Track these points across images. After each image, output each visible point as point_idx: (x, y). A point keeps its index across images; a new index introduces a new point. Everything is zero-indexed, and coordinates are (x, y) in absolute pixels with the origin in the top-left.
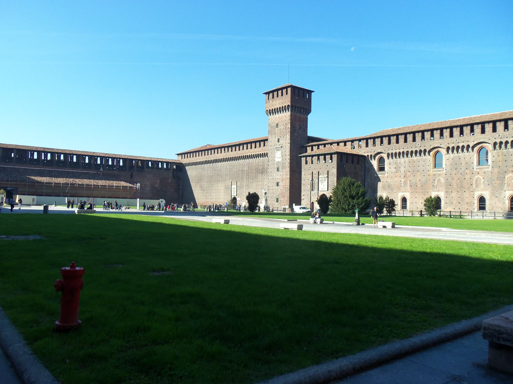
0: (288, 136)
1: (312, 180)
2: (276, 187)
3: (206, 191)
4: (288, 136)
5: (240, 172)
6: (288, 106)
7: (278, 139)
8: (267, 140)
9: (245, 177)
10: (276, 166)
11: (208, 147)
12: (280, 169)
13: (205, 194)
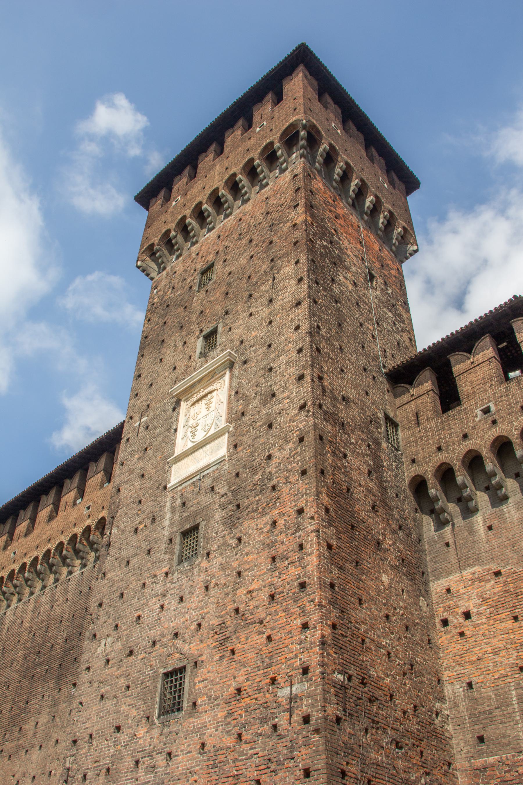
4: (288, 269)
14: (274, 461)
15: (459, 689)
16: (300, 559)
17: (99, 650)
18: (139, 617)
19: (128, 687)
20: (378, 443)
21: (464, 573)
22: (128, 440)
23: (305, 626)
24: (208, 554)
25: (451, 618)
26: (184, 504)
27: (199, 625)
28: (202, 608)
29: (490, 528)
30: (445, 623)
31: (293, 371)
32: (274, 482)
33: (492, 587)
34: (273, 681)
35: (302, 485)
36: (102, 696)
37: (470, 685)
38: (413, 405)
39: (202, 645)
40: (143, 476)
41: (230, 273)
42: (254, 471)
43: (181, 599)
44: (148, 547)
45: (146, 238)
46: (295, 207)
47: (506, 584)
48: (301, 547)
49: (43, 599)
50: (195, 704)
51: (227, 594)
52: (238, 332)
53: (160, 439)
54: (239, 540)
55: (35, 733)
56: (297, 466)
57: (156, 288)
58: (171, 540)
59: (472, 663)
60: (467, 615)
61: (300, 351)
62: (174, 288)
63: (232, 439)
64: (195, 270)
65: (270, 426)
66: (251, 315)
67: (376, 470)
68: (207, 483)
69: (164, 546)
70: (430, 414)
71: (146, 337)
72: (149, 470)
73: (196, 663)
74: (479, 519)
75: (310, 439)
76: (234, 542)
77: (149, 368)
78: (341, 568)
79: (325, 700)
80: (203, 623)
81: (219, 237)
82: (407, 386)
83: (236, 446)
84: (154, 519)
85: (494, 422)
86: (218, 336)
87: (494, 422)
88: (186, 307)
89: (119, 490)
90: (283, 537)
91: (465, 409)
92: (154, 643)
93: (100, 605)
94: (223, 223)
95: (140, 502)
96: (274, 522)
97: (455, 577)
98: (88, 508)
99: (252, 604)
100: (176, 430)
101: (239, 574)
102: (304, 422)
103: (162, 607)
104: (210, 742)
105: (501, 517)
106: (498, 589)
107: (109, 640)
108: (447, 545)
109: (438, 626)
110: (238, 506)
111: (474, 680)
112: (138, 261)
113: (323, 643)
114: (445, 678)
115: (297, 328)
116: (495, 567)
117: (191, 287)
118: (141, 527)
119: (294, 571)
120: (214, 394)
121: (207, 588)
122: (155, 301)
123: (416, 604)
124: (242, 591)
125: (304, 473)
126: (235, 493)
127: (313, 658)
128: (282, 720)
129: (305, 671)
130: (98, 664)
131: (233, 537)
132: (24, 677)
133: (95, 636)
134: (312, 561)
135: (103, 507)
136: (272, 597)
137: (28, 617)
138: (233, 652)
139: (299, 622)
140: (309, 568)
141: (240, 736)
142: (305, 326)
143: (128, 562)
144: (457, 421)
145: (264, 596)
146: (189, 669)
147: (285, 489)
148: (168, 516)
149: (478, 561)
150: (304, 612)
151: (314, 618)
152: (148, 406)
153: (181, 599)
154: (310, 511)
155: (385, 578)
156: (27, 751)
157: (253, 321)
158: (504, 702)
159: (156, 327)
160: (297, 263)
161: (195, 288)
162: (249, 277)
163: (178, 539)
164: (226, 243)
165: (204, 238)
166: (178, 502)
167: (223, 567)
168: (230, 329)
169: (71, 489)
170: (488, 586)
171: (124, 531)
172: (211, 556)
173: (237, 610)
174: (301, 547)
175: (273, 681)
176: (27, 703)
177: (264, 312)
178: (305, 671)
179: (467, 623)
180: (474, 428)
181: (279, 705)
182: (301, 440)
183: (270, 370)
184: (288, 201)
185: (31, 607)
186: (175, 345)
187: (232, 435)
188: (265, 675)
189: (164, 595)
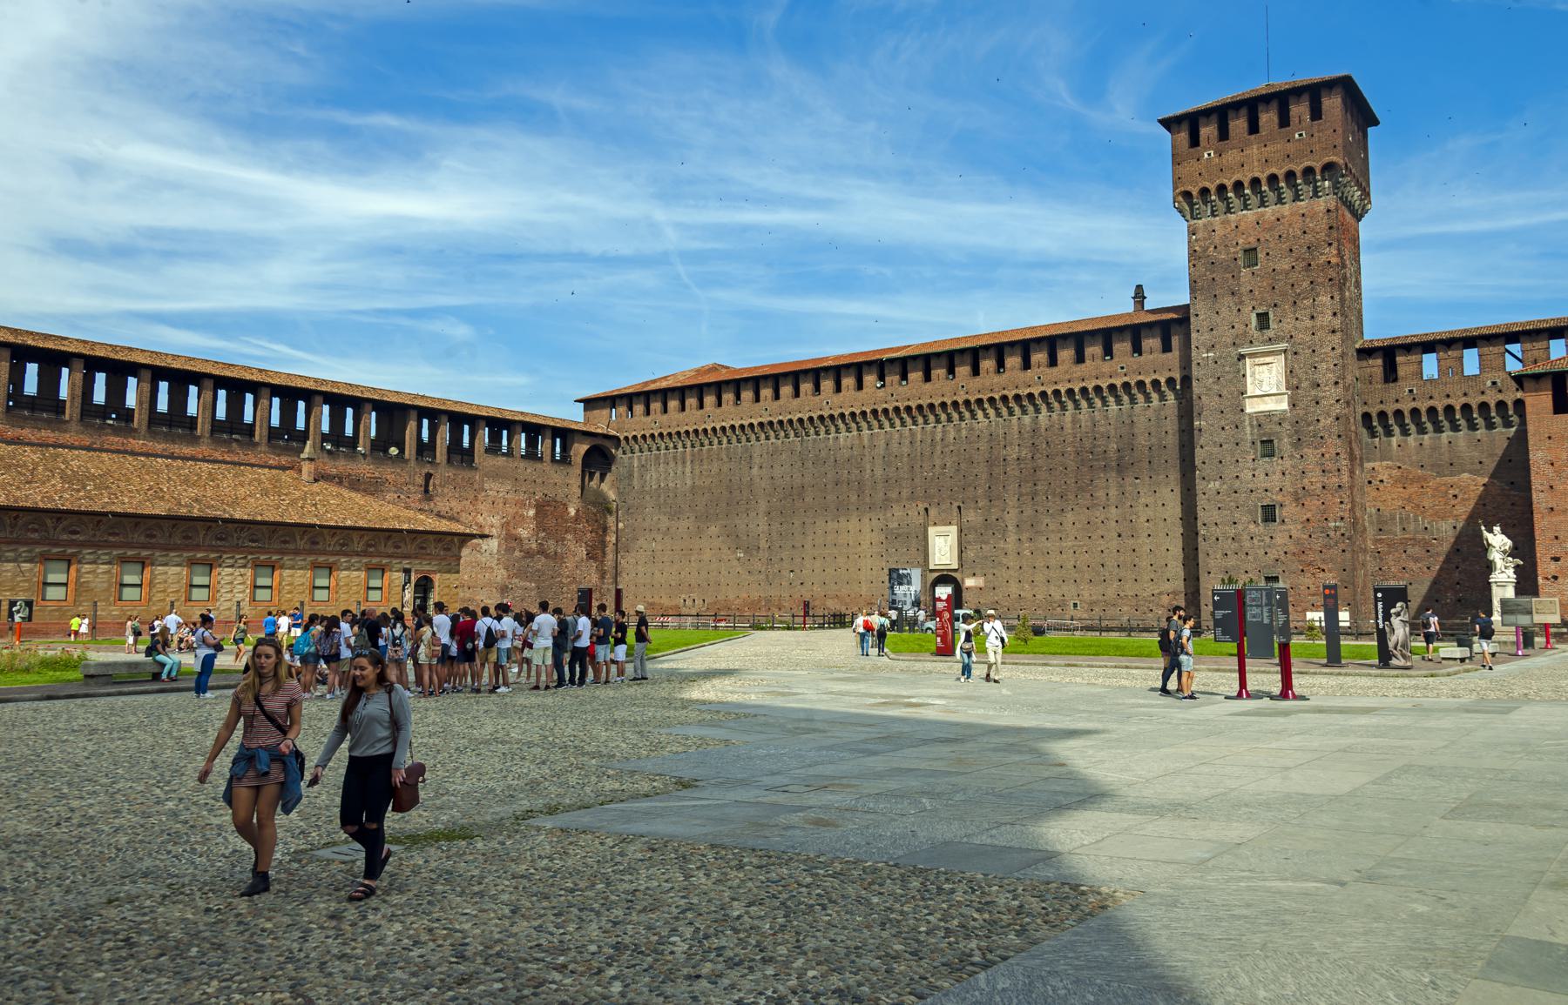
0: (1324, 299)
2: (1260, 529)
3: (764, 555)
4: (1324, 299)
5: (982, 470)
6: (1329, 167)
9: (1013, 487)
10: (1248, 433)
11: (724, 376)
12: (1284, 444)
13: (758, 566)
31: (1332, 377)
33: (1395, 472)
45: (1177, 180)
52: (1288, 325)
56: (1335, 430)
68: (1276, 419)
72: (1224, 393)
74: (1394, 440)
126: (1296, 432)
127: (1346, 515)
128: (1332, 534)
134: (1345, 478)
144: (1393, 390)
145: (1319, 485)
149: (1390, 459)
154: (1343, 456)
158: (1393, 518)
161: (1240, 262)
177: (1309, 323)
187: (1290, 398)
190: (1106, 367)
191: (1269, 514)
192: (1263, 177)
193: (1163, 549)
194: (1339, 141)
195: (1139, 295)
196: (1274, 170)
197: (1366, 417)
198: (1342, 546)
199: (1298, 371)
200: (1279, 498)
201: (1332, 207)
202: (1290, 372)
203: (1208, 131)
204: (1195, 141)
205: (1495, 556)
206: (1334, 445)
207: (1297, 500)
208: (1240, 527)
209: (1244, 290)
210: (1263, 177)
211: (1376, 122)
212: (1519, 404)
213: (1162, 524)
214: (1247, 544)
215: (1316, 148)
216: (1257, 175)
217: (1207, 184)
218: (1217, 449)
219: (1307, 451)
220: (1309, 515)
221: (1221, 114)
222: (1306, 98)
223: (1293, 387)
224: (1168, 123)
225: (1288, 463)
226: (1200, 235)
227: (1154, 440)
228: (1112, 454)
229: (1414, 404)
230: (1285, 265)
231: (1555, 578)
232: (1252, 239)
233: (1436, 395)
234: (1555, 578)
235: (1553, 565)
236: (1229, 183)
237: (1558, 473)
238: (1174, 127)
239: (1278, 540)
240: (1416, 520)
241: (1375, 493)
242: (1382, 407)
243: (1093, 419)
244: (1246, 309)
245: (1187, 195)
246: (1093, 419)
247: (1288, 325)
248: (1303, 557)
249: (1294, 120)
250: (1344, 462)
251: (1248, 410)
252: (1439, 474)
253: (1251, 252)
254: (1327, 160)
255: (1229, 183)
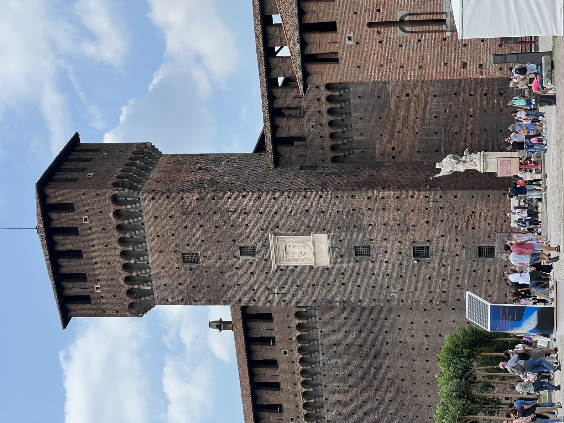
0: (230, 204)
1: (401, 23)
4: (230, 204)
6: (115, 199)
7: (244, 250)
8: (244, 308)
10: (348, 265)
12: (358, 238)
14: (341, 210)
15: (419, 155)
16: (388, 198)
17: (396, 296)
18: (387, 275)
19: (415, 275)
20: (320, 173)
21: (376, 147)
22: (284, 301)
23: (412, 197)
24: (371, 240)
25: (393, 155)
26: (341, 256)
27: (400, 242)
28: (393, 241)
29: (361, 134)
30: (394, 157)
32: (351, 209)
34: (427, 209)
35: (357, 197)
36: (416, 289)
37: (418, 152)
38: (293, 157)
39: (408, 239)
40: (314, 285)
41: (202, 241)
42: (342, 219)
43: (386, 252)
44: (355, 274)
46: (182, 198)
47: (386, 133)
48: (383, 198)
49: (329, 386)
50: (428, 241)
51: (391, 230)
52: (253, 232)
53: (296, 277)
54: (370, 225)
55: (407, 367)
56: (347, 199)
57: (167, 300)
58: (357, 261)
59: (411, 150)
60: (393, 149)
61: (289, 197)
62: (180, 284)
63: (319, 232)
64: (177, 268)
65: (322, 212)
66: (247, 225)
67: (336, 174)
68: (336, 244)
69: (358, 265)
70: (302, 150)
71: (210, 301)
72: (311, 282)
73: (414, 242)
74: (356, 138)
75: (338, 193)
76: (370, 227)
77: (239, 294)
78: (390, 186)
79: (437, 190)
80: (399, 240)
81: (160, 251)
82: (282, 158)
83: (324, 230)
84: (342, 274)
85: (320, 124)
86: (248, 245)
87: (320, 124)
88: (206, 272)
89: (315, 301)
90: (376, 206)
91: (308, 135)
92: (401, 264)
93: (374, 300)
94: (149, 250)
95: (328, 284)
96: (369, 209)
97: (377, 151)
98: (285, 353)
99: (398, 218)
100: (296, 267)
101: (384, 224)
102: (329, 196)
103: (386, 262)
104: (442, 233)
105: (357, 130)
106: (386, 136)
107: (392, 291)
108: (362, 152)
109: (394, 160)
110: (355, 226)
111: (417, 150)
112: (138, 316)
113: (419, 190)
114: (414, 160)
115: (274, 198)
116: (378, 135)
117: (191, 269)
118: (343, 281)
119: (391, 201)
120: (287, 244)
121: (385, 239)
122: (180, 298)
123: (389, 166)
124: (392, 223)
125: (353, 196)
126: (348, 228)
127: (423, 193)
128: (440, 205)
129: (426, 197)
130: (402, 295)
131: (368, 228)
132: (374, 386)
133: (388, 300)
134: (390, 193)
135: (290, 339)
136: (398, 210)
137: (337, 396)
138: (413, 226)
139: (410, 199)
140: (392, 195)
141: (441, 221)
142: (277, 195)
143: (359, 286)
145: (396, 213)
146: (415, 245)
147: (357, 204)
148: (343, 265)
149: (373, 142)
150: (407, 197)
151: (410, 193)
152: (268, 289)
153: (386, 252)
155: (385, 174)
156: (414, 371)
157: (251, 224)
159: (207, 294)
160: (229, 198)
161: (194, 266)
162: (216, 227)
163: (358, 258)
164: (172, 245)
165: (150, 265)
166: (339, 260)
167: (379, 232)
168: (248, 237)
169: (263, 373)
170: (385, 139)
171: (340, 292)
172: (372, 238)
173: (399, 225)
174: (383, 198)
175: (427, 209)
176: (389, 379)
177: (251, 216)
178: (426, 197)
179: (396, 149)
180: (319, 133)
181: (435, 206)
182: (337, 197)
183: (291, 212)
184: (173, 203)
185: (330, 396)
186: (233, 276)
188: (424, 212)
189: (382, 261)
190: (283, 364)
191: (421, 252)
192: (120, 248)
193: (452, 324)
194: (94, 191)
195: (221, 325)
196: (115, 241)
197: (334, 160)
198: (451, 198)
199: (294, 225)
200: (407, 244)
201: (151, 196)
202: (294, 231)
203: (74, 289)
204: (86, 299)
205: (461, 168)
206: (361, 199)
207: (409, 230)
208: (433, 274)
209: (219, 264)
210: (120, 248)
211: (76, 137)
212: (329, 87)
213: (428, 325)
214: (449, 270)
215: (97, 208)
216: (118, 253)
217: (124, 290)
218: (362, 290)
219: (366, 220)
220: (423, 222)
221: (60, 278)
222: (54, 215)
223: (308, 230)
224: (65, 321)
225: (376, 236)
226: (168, 295)
227: (352, 328)
228: (364, 362)
229: (325, 125)
230: (198, 233)
231: (481, 66)
232: (175, 256)
233: (318, 109)
234: (481, 66)
235: (470, 67)
236: (125, 274)
237: (390, 62)
238: (70, 314)
239: (446, 245)
240: (428, 124)
241: (404, 154)
242: (327, 148)
243: (331, 376)
244: (236, 262)
245: (131, 306)
246: (331, 376)
247: (253, 232)
248: (461, 227)
249: (72, 224)
250: (376, 194)
251: (327, 263)
252: (388, 105)
253: (186, 258)
254: (109, 201)
255: (125, 274)
